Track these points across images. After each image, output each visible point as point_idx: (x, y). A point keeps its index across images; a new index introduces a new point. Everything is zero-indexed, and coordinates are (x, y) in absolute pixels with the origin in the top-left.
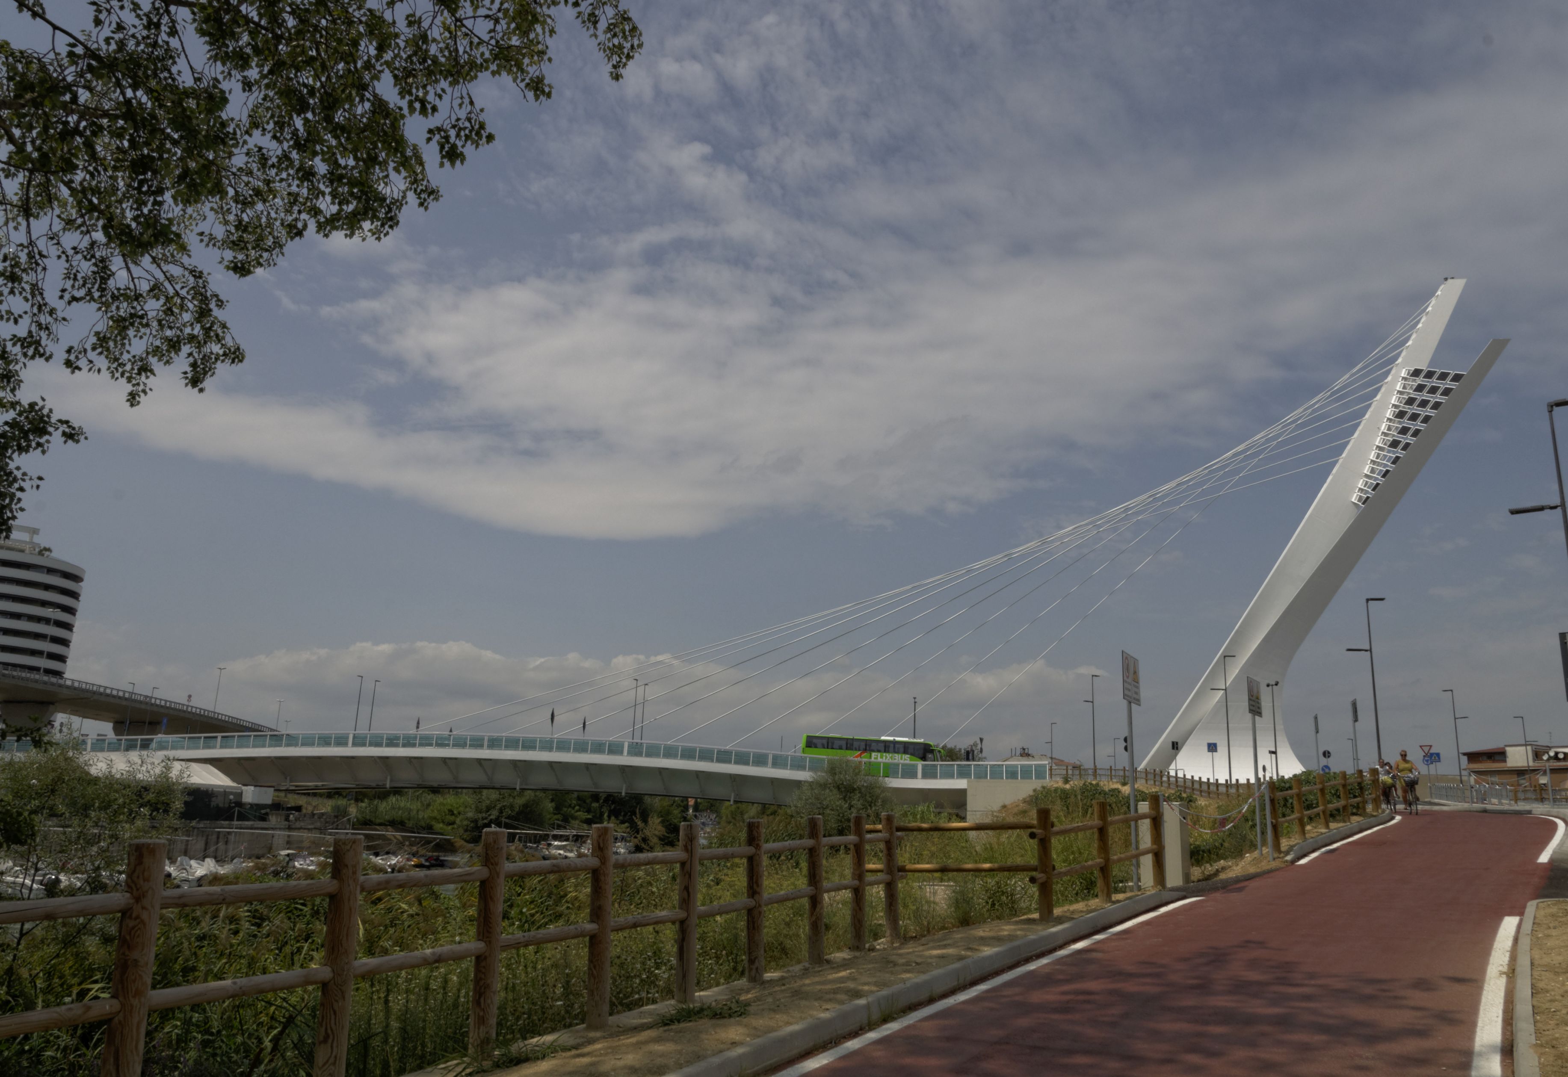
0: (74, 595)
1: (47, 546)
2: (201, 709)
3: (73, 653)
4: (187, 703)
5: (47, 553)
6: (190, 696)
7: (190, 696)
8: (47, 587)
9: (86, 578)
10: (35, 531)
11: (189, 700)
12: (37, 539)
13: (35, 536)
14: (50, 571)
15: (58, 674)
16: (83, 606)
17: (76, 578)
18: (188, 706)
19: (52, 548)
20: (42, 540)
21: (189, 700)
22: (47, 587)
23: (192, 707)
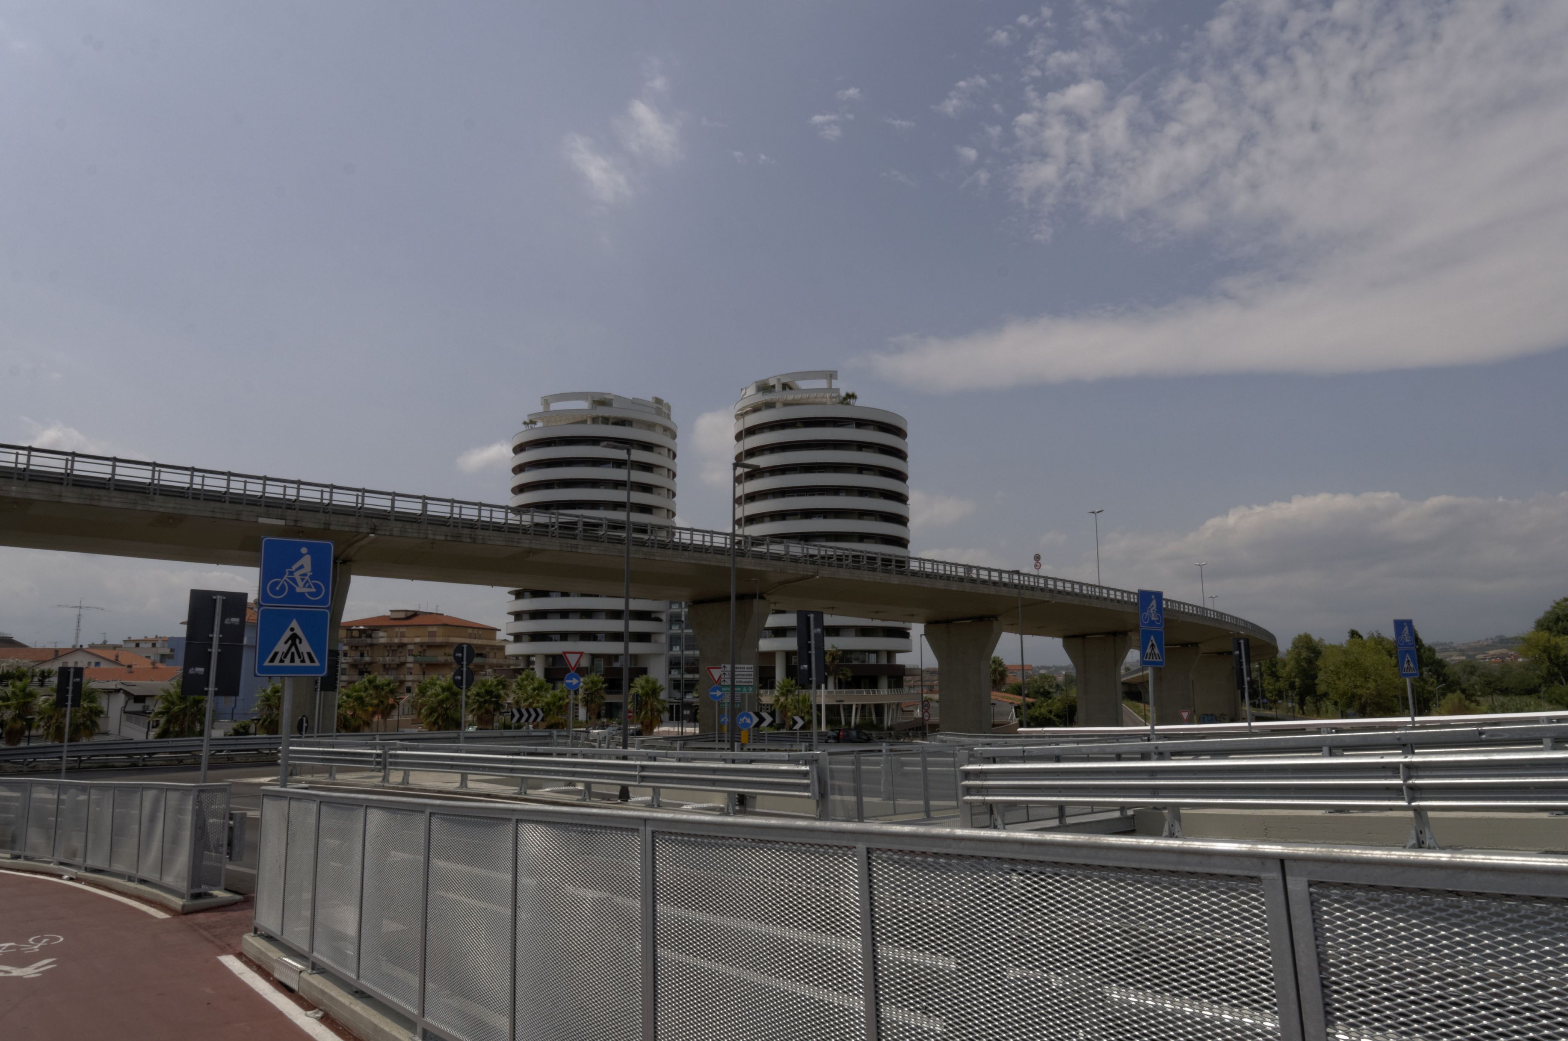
0: (901, 455)
1: (850, 393)
2: (1073, 583)
3: (914, 530)
4: (1035, 572)
5: (851, 401)
6: (1037, 558)
7: (1037, 558)
8: (861, 446)
9: (910, 431)
10: (831, 375)
11: (1037, 566)
12: (835, 384)
13: (834, 381)
14: (861, 423)
15: (901, 563)
16: (912, 467)
17: (899, 432)
18: (1038, 577)
19: (857, 394)
20: (843, 387)
21: (1037, 566)
22: (861, 446)
23: (1046, 579)
